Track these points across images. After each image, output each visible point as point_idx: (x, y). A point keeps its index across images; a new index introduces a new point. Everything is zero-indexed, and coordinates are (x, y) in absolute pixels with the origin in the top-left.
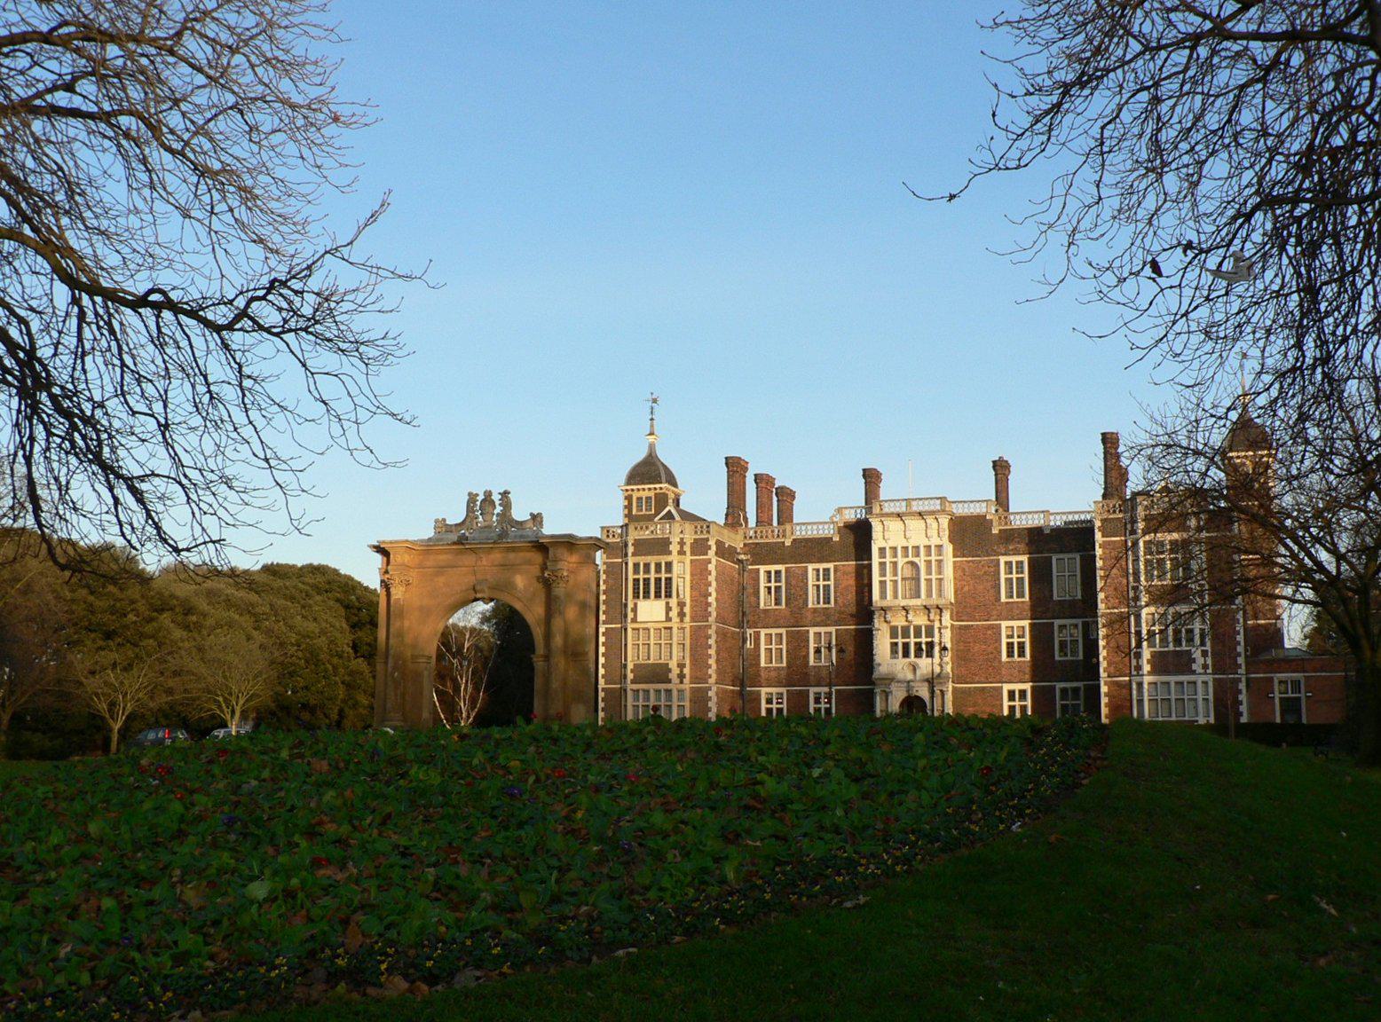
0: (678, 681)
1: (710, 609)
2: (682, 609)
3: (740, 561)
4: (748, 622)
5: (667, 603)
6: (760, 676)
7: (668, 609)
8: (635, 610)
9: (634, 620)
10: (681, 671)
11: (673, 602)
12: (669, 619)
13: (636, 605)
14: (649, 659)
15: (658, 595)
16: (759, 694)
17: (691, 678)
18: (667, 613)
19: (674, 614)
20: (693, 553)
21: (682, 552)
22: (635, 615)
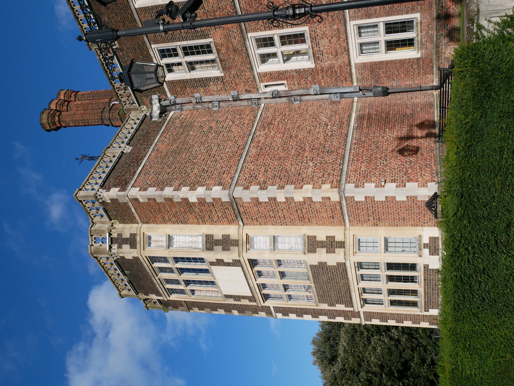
0: (340, 252)
1: (209, 200)
2: (217, 243)
3: (164, 111)
4: (248, 91)
5: (212, 264)
6: (331, 67)
7: (220, 262)
8: (238, 298)
9: (252, 299)
10: (322, 244)
11: (210, 256)
12: (236, 263)
13: (227, 297)
14: (309, 287)
15: (206, 271)
16: (363, 66)
17: (332, 224)
18: (228, 264)
19: (227, 257)
20: (132, 220)
21: (132, 241)
22: (244, 297)
